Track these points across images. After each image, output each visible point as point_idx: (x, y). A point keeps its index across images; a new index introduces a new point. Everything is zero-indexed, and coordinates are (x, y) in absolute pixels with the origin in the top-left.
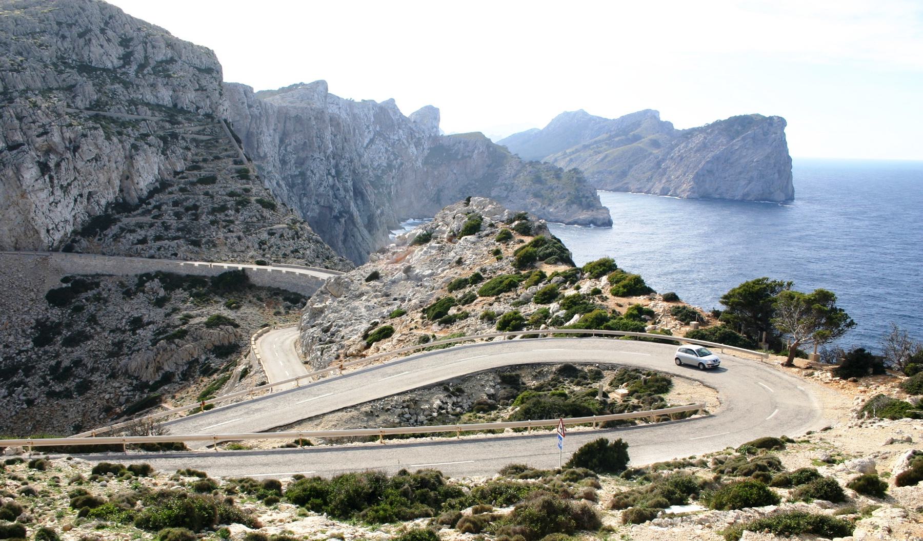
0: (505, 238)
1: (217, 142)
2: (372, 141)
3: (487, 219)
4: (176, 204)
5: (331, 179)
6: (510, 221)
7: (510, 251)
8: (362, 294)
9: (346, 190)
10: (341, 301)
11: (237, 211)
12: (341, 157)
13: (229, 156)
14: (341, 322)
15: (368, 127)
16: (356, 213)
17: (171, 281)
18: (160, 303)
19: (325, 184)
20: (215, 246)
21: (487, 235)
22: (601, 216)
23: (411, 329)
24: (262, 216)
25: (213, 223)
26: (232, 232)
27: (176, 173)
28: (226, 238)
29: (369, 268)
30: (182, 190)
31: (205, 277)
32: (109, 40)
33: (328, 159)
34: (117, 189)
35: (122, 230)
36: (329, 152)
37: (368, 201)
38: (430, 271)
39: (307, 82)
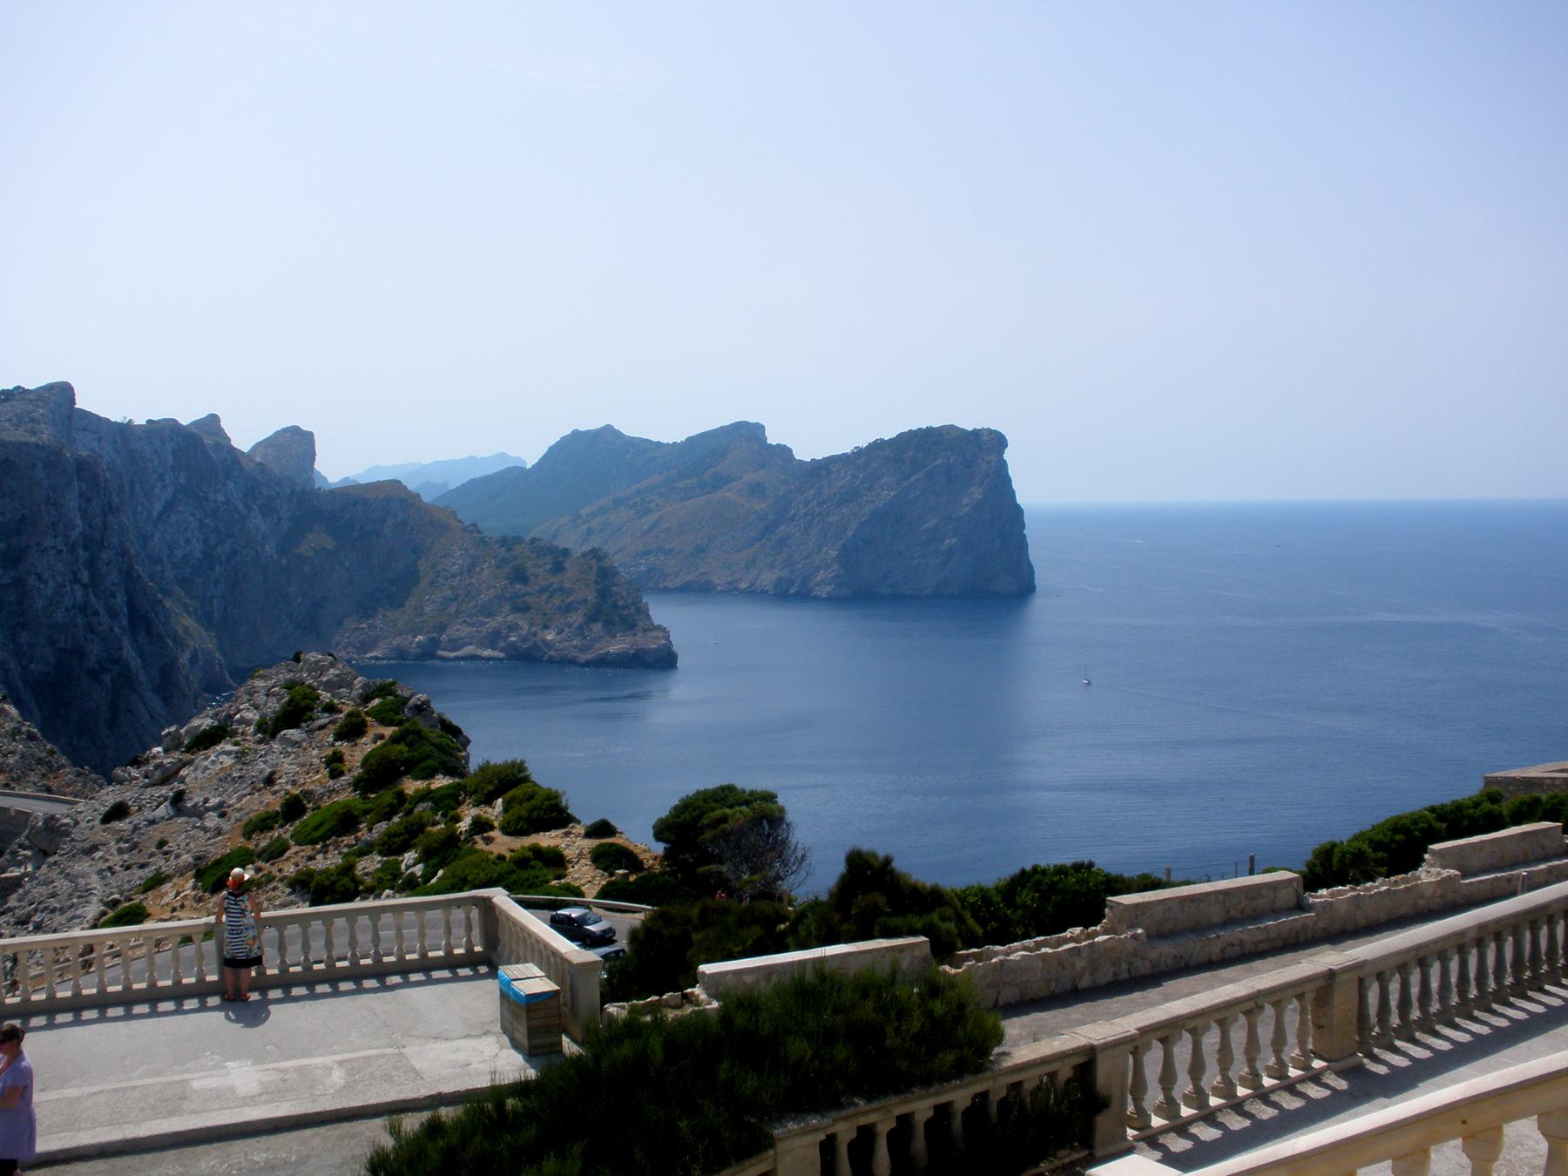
0: (352, 730)
2: (169, 506)
3: (326, 696)
5: (79, 593)
6: (366, 698)
7: (357, 754)
8: (95, 848)
9: (113, 614)
10: (55, 863)
14: (54, 903)
15: (161, 477)
16: (135, 662)
21: (322, 727)
22: (652, 643)
23: (174, 910)
29: (110, 796)
33: (72, 550)
36: (75, 534)
38: (217, 800)
39: (31, 385)
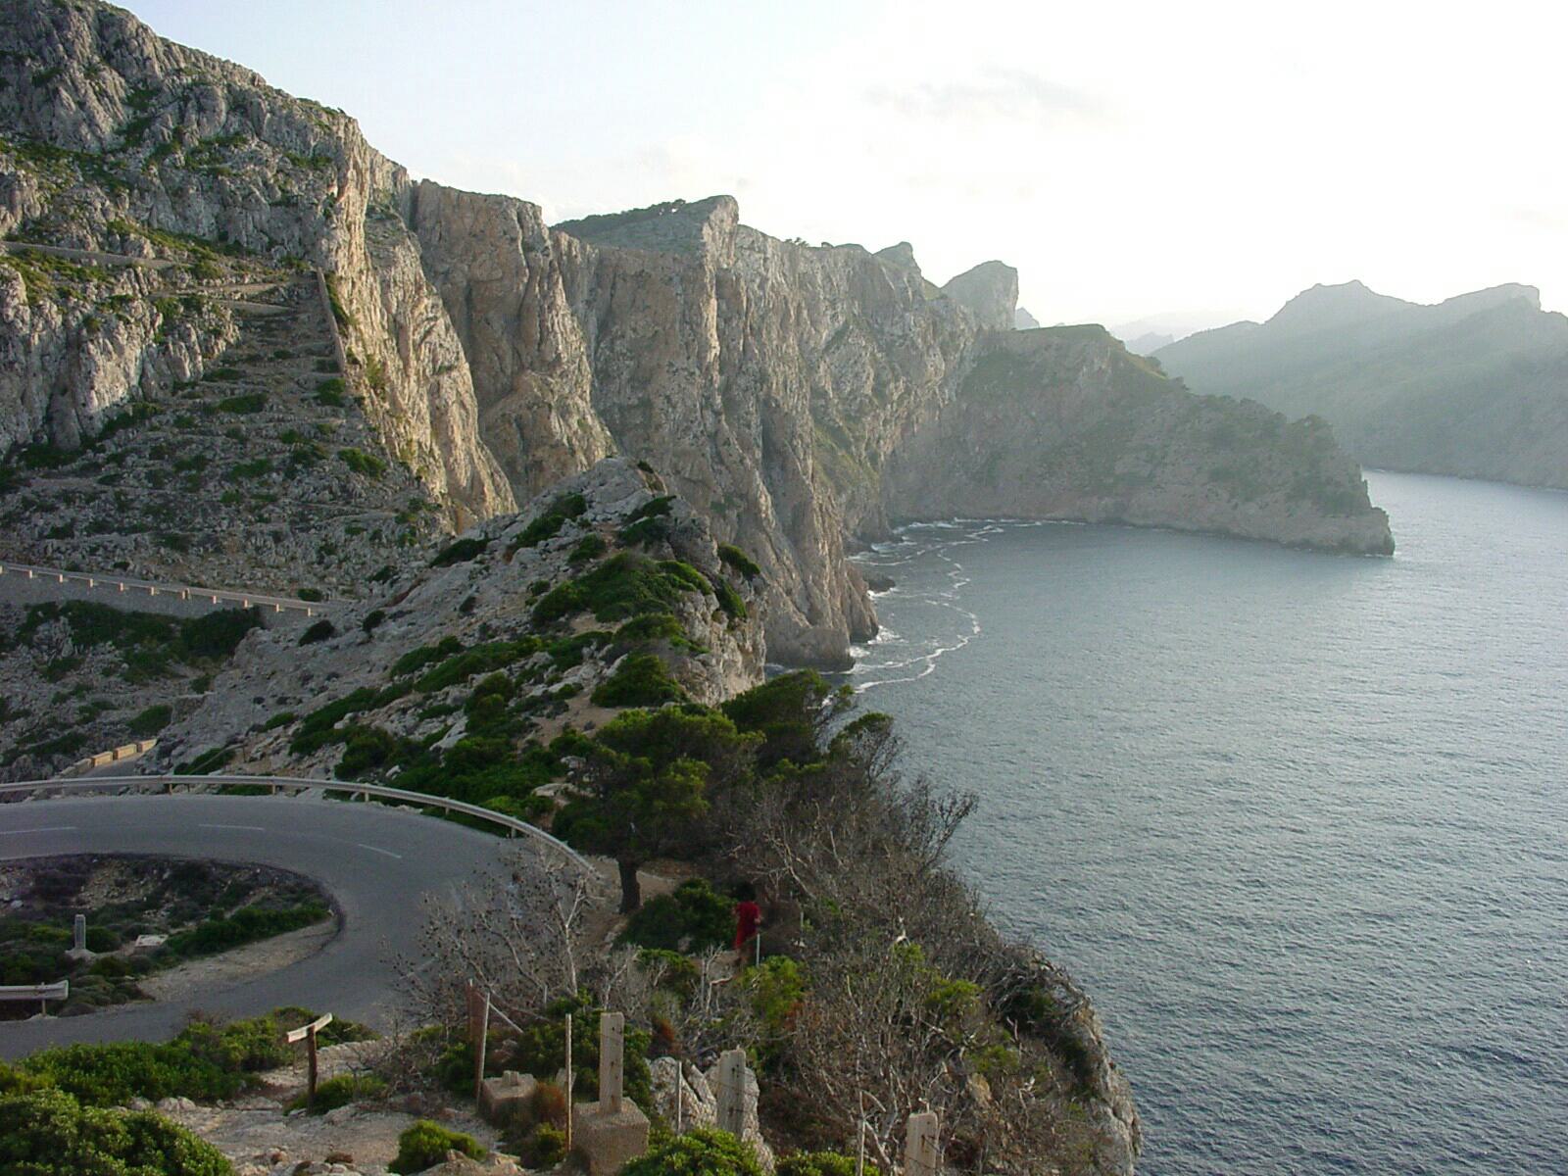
1: (295, 319)
2: (839, 336)
4: (157, 453)
5: (710, 418)
11: (291, 474)
12: (740, 371)
13: (310, 352)
15: (833, 304)
16: (765, 501)
17: (93, 622)
18: (55, 671)
19: (696, 429)
20: (218, 550)
24: (344, 489)
25: (228, 500)
26: (267, 521)
27: (178, 386)
28: (249, 535)
30: (180, 422)
31: (173, 619)
32: (101, 94)
34: (40, 415)
35: (27, 504)
37: (795, 472)
39: (690, 199)
